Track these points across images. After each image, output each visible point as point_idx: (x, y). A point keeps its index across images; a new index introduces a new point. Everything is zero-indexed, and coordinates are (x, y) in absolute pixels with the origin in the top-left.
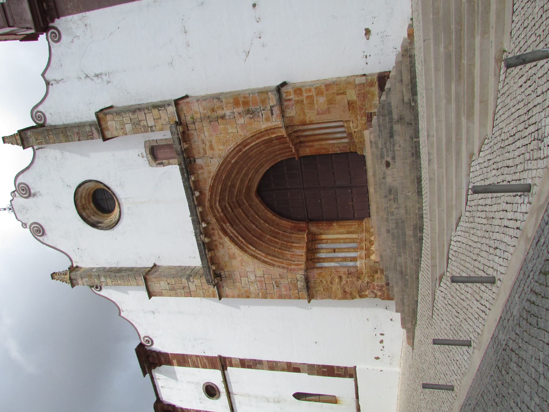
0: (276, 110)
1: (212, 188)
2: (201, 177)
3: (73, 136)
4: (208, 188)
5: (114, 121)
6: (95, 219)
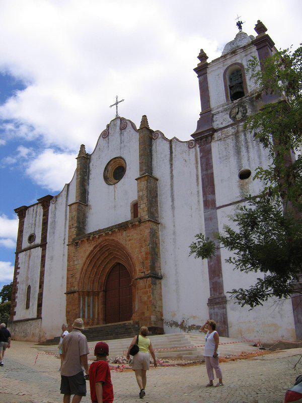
0: (143, 275)
1: (113, 240)
2: (118, 234)
4: (113, 238)
6: (110, 168)
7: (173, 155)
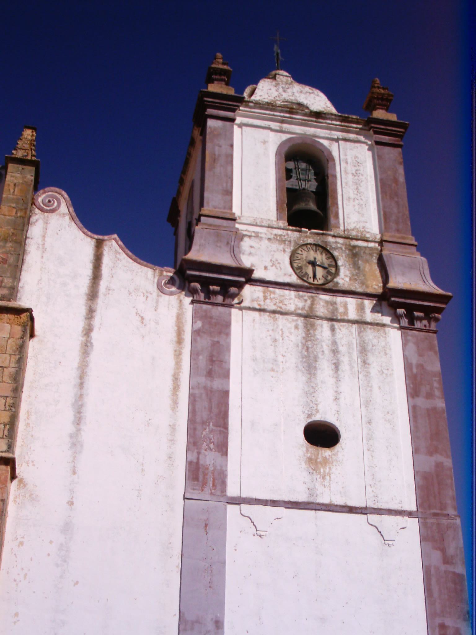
3: (4, 250)
5: (8, 336)
7: (103, 285)
